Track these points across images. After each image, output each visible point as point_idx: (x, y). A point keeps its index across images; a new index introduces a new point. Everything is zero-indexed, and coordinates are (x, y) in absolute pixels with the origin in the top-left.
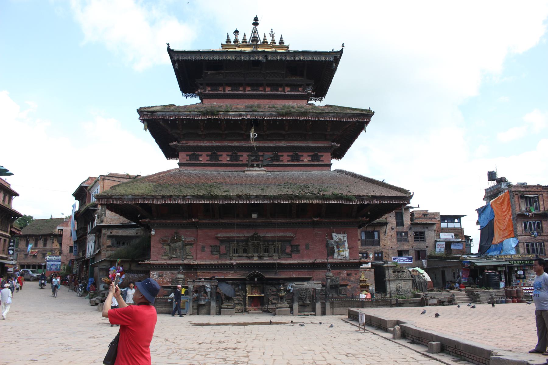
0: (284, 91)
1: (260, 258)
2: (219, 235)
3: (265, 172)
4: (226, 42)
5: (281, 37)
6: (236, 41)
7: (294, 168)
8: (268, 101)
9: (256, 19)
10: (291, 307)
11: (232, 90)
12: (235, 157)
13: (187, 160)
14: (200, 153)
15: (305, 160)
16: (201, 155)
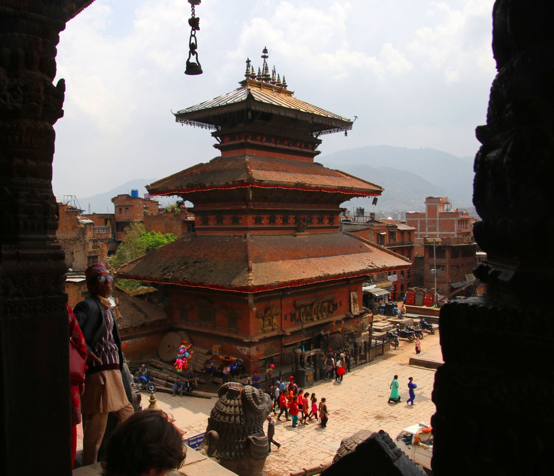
0: (300, 147)
1: (318, 318)
2: (298, 303)
3: (307, 236)
4: (246, 76)
5: (284, 79)
6: (253, 77)
7: (320, 230)
8: (290, 156)
9: (265, 51)
10: (356, 360)
11: (266, 142)
12: (285, 221)
13: (253, 224)
14: (262, 216)
15: (326, 222)
16: (263, 218)
